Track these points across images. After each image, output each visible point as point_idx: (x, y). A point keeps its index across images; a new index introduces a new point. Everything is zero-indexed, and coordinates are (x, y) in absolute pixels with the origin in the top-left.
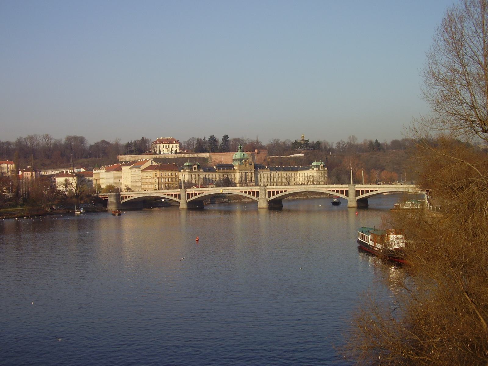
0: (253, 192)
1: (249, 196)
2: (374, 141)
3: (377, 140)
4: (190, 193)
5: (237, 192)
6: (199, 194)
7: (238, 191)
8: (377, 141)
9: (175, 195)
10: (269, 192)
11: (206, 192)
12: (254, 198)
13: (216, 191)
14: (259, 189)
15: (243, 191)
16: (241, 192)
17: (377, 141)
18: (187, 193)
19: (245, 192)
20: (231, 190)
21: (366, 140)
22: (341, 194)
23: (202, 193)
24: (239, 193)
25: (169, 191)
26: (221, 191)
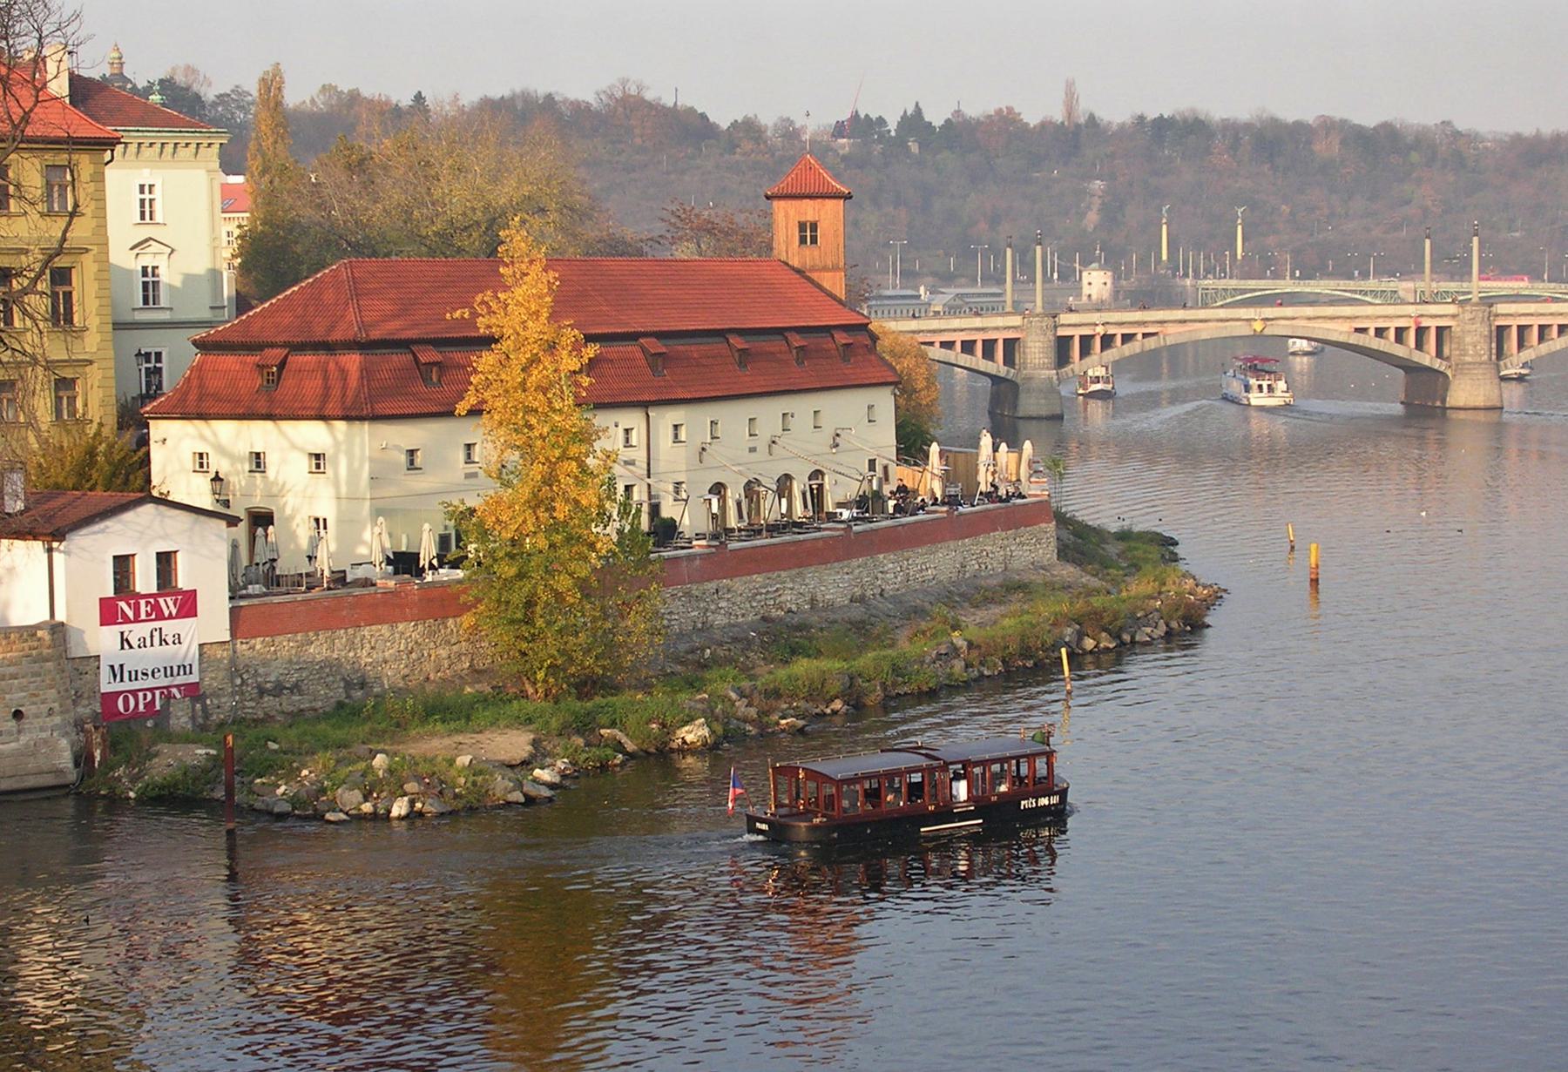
0: (1421, 332)
1: (1399, 351)
2: (406, 101)
3: (420, 93)
4: (1077, 333)
5: (1341, 333)
6: (1127, 338)
7: (1346, 327)
8: (419, 97)
9: (989, 348)
10: (1501, 330)
11: (1171, 329)
12: (1427, 358)
13: (1227, 324)
14: (1454, 316)
15: (1372, 326)
16: (1357, 330)
17: (419, 97)
18: (1061, 332)
19: (1380, 332)
20: (1309, 319)
21: (660, 99)
22: (962, 352)
23: (1145, 335)
24: (1349, 333)
25: (956, 323)
26: (1258, 326)
